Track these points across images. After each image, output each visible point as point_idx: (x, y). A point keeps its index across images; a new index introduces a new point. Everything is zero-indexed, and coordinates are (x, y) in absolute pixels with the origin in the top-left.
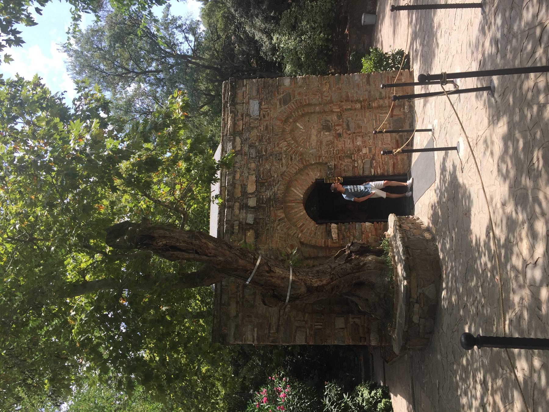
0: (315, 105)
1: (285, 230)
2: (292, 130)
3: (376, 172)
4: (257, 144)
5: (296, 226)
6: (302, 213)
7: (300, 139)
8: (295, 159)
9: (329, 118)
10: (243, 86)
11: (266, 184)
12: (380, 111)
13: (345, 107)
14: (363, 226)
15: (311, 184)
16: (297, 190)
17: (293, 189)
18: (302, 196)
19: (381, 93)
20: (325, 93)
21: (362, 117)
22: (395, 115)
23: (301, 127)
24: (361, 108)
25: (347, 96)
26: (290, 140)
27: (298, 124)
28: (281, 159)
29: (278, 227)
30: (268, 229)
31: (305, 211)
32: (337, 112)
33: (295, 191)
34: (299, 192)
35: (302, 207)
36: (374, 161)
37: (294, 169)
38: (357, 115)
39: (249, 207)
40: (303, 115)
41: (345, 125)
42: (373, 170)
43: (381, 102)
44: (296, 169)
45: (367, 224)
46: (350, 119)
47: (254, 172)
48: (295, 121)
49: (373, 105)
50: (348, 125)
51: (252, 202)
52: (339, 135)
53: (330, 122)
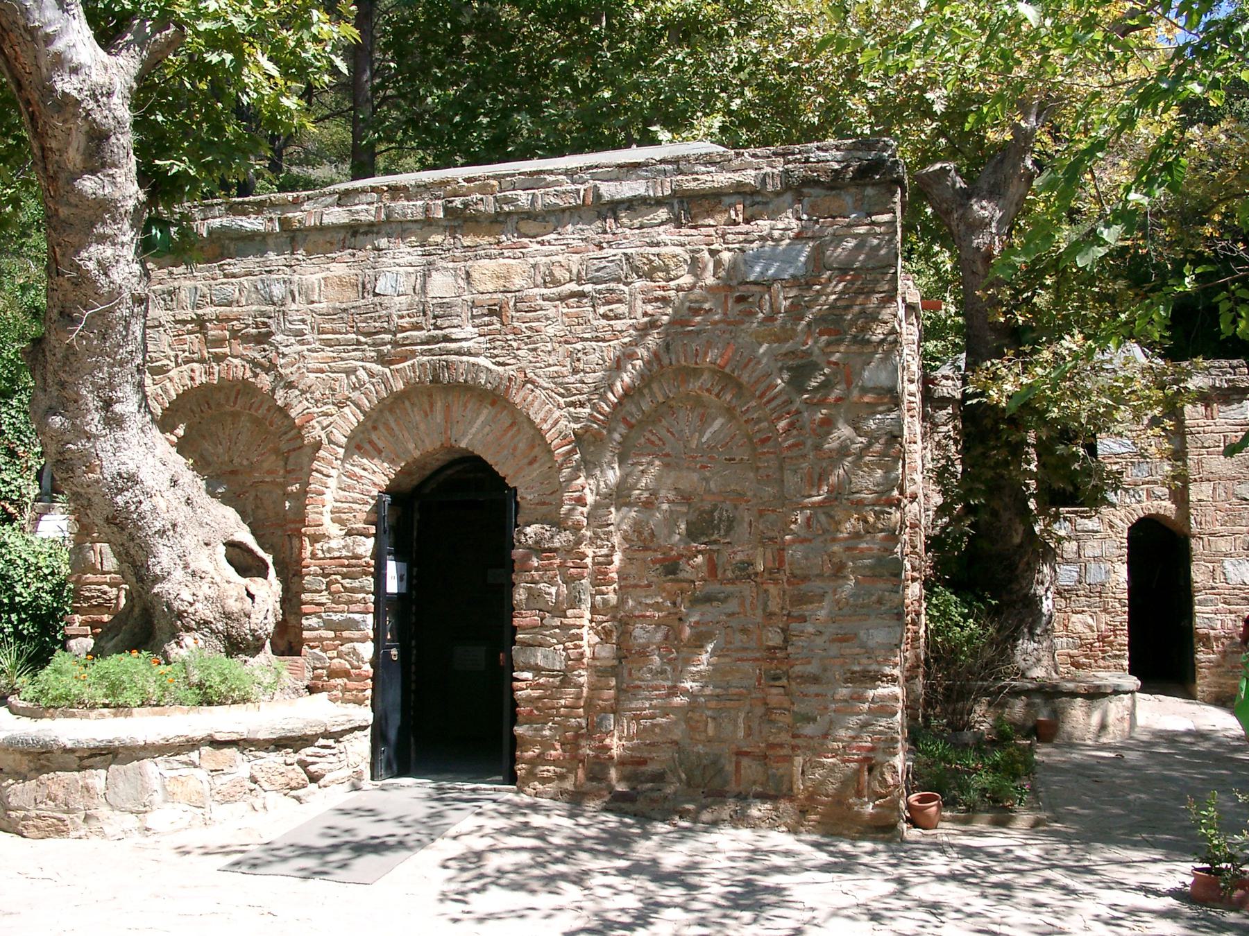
1: (355, 395)
2: (698, 402)
3: (523, 685)
4: (639, 284)
5: (375, 428)
6: (411, 446)
7: (663, 433)
8: (576, 419)
9: (742, 530)
11: (498, 326)
13: (773, 590)
14: (357, 634)
15: (501, 474)
16: (484, 424)
17: (485, 412)
18: (463, 445)
19: (810, 719)
20: (823, 518)
21: (737, 650)
22: (738, 764)
23: (707, 435)
24: (769, 648)
25: (801, 599)
26: (653, 394)
27: (717, 424)
28: (575, 371)
29: (362, 374)
30: (359, 343)
31: (417, 454)
33: (479, 422)
34: (475, 434)
35: (432, 443)
37: (542, 415)
38: (744, 631)
39: (426, 276)
41: (714, 587)
42: (528, 675)
44: (545, 421)
45: (367, 650)
46: (733, 605)
47: (539, 280)
48: (729, 411)
49: (774, 691)
51: (442, 285)
52: (671, 568)
53: (727, 534)
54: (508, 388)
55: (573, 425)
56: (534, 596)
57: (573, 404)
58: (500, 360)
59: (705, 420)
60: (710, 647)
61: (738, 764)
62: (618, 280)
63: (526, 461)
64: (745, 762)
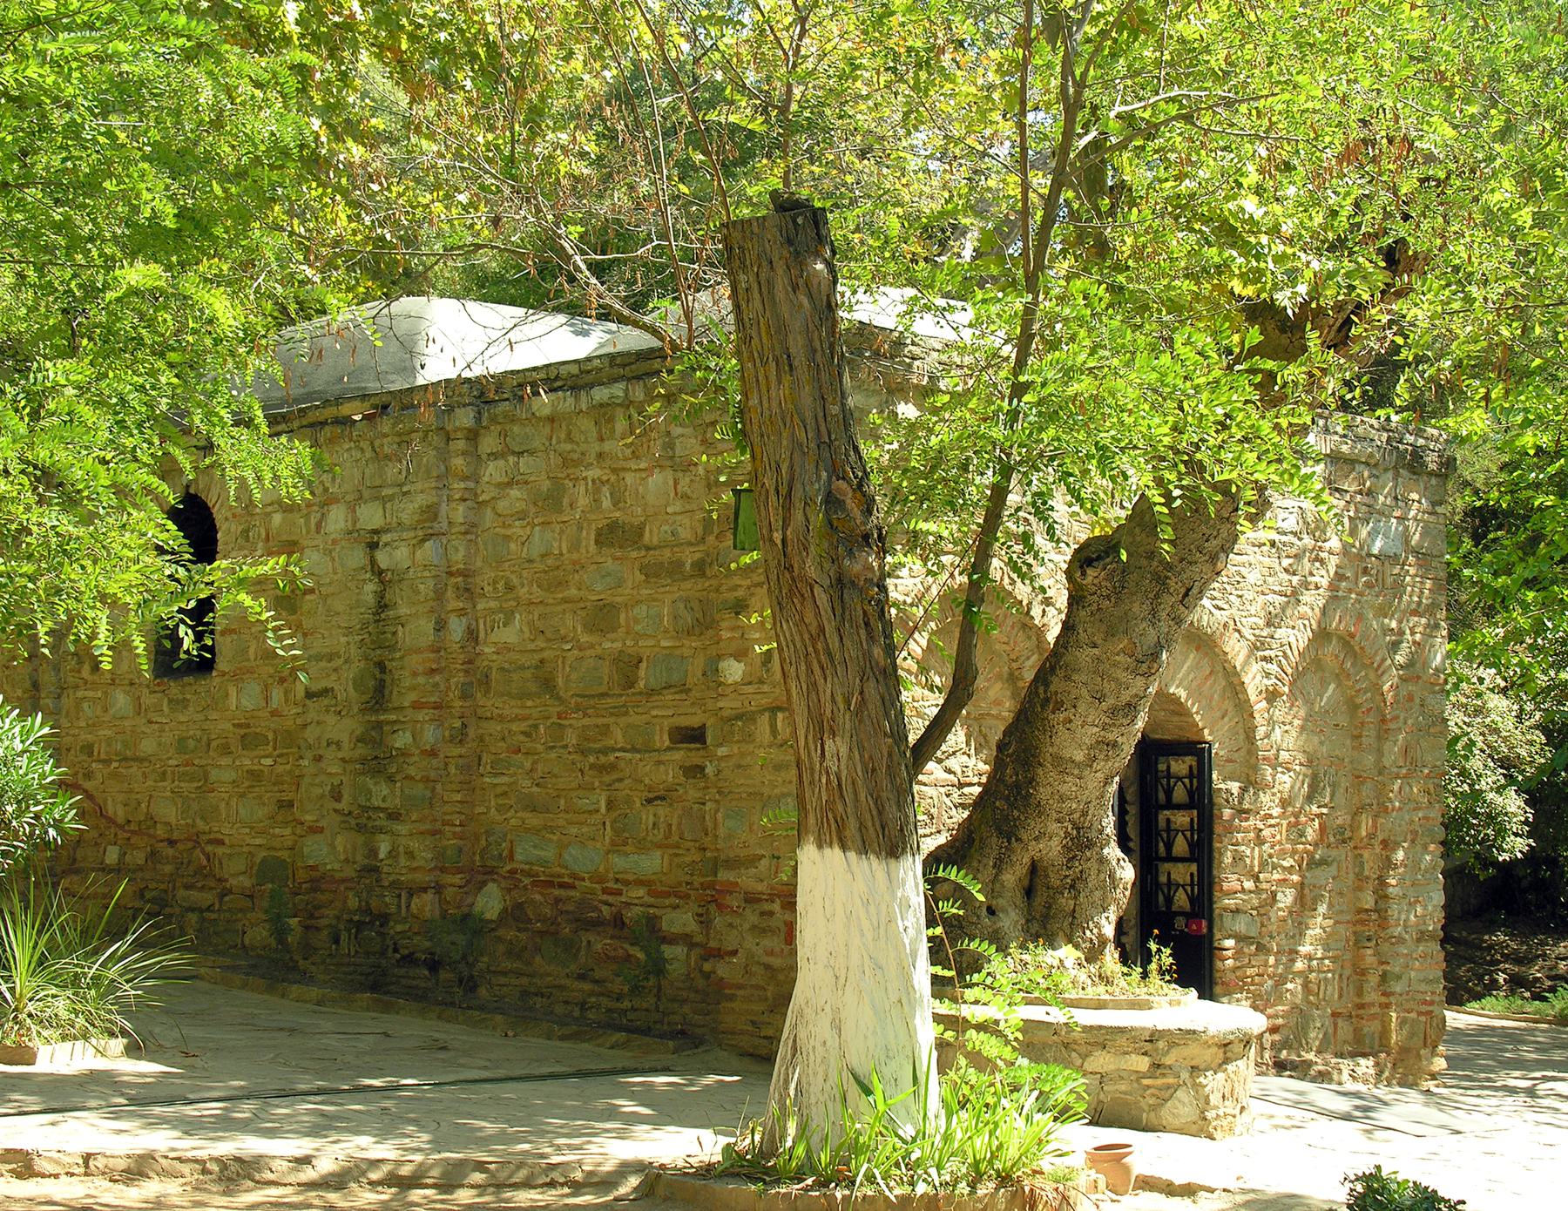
0: (1380, 753)
8: (1268, 675)
10: (1434, 504)
12: (1347, 972)
13: (1366, 854)
16: (1190, 669)
19: (1399, 977)
22: (1335, 1025)
24: (1360, 911)
27: (1332, 686)
32: (1354, 827)
36: (1253, 948)
40: (1353, 707)
43: (1373, 979)
46: (1333, 870)
48: (1340, 676)
50: (1323, 862)
54: (1222, 634)
55: (1265, 681)
56: (1238, 858)
57: (1264, 659)
58: (1220, 603)
59: (1324, 684)
60: (1322, 909)
61: (1335, 1025)
62: (1295, 534)
63: (1218, 714)
64: (1340, 1021)
